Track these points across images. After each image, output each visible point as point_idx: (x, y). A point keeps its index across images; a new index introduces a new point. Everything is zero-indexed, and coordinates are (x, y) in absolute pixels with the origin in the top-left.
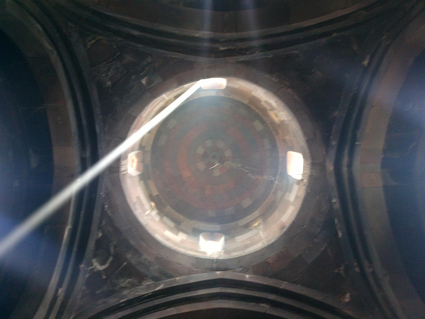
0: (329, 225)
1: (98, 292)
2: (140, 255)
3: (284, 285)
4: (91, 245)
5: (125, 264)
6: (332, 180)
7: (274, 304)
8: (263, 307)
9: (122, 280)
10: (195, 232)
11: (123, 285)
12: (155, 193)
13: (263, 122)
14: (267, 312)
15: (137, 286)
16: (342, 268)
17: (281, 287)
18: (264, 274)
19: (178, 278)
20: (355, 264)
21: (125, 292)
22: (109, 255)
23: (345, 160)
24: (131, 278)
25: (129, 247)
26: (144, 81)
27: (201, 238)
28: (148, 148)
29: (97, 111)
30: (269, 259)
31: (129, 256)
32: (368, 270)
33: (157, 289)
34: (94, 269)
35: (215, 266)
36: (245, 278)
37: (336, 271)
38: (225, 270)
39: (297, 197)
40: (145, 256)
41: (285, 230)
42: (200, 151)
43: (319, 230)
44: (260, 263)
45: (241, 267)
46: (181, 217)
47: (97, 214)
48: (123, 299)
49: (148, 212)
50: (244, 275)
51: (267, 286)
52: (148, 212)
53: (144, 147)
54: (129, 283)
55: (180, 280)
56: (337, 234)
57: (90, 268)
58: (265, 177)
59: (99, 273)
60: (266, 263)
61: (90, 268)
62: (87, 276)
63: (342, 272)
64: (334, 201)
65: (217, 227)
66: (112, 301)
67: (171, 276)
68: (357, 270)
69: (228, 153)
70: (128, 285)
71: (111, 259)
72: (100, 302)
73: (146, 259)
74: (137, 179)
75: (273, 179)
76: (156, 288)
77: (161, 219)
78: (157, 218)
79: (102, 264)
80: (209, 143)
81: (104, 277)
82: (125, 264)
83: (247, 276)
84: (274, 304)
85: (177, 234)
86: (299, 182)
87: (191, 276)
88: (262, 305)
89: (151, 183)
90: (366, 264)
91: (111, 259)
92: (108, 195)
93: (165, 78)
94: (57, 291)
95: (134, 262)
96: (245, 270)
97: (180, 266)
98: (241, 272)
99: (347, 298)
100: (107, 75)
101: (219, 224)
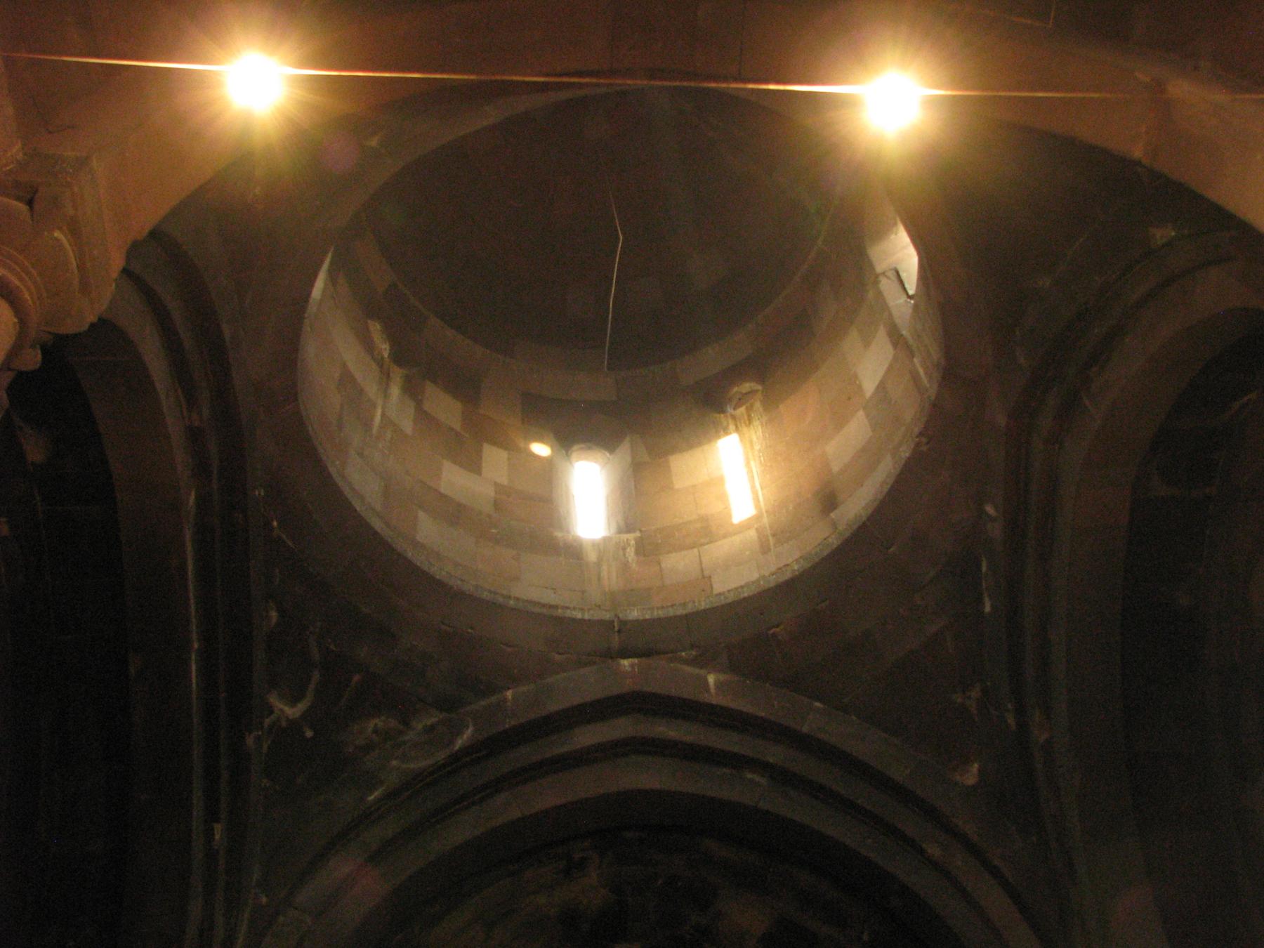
3: (814, 719)
5: (356, 678)
7: (782, 777)
14: (763, 805)
15: (401, 733)
16: (975, 693)
17: (805, 729)
19: (509, 694)
20: (1009, 706)
30: (777, 626)
33: (459, 743)
34: (279, 719)
35: (616, 641)
37: (958, 698)
43: (932, 574)
45: (692, 646)
50: (702, 672)
54: (376, 731)
56: (979, 601)
61: (267, 721)
68: (1011, 720)
71: (316, 676)
76: (451, 742)
79: (294, 701)
82: (356, 678)
84: (782, 777)
87: (549, 680)
88: (749, 776)
91: (316, 676)
94: (209, 833)
96: (705, 659)
97: (509, 650)
98: (692, 662)
99: (971, 776)
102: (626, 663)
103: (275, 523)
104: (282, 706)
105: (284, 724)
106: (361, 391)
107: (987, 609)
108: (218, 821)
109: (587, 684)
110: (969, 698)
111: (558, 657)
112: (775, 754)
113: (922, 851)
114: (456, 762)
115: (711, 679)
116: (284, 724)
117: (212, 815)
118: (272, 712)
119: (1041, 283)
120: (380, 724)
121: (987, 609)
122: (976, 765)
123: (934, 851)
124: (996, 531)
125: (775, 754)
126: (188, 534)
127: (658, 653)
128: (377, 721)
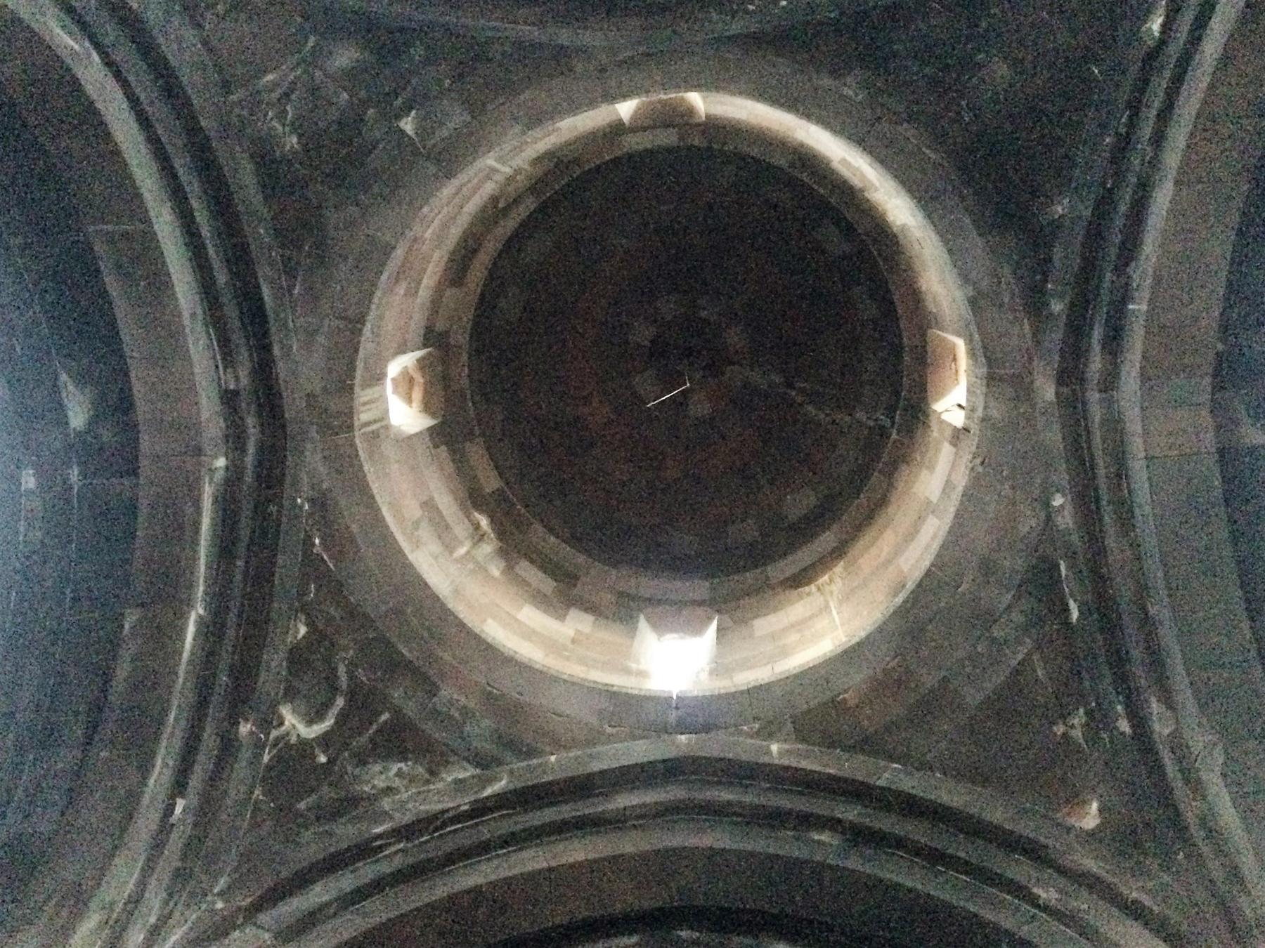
0: (1041, 582)
1: (302, 806)
2: (433, 691)
3: (890, 775)
4: (275, 661)
5: (385, 717)
6: (1054, 437)
7: (859, 836)
8: (819, 842)
9: (377, 768)
10: (623, 610)
11: (380, 783)
12: (491, 483)
13: (849, 230)
15: (428, 782)
16: (1079, 718)
18: (831, 742)
19: (553, 758)
21: (386, 804)
22: (334, 690)
23: (1096, 364)
24: (405, 760)
25: (395, 665)
26: (408, 125)
27: (643, 624)
28: (461, 338)
29: (260, 234)
30: (846, 691)
31: (397, 695)
32: (1161, 728)
33: (488, 792)
35: (673, 717)
36: (769, 753)
37: (1059, 729)
38: (706, 728)
39: (948, 485)
40: (447, 692)
41: (899, 600)
42: (643, 334)
44: (815, 709)
45: (756, 719)
46: (581, 559)
47: (287, 563)
48: (376, 822)
49: (462, 551)
50: (765, 743)
51: (832, 778)
52: (462, 551)
53: (445, 334)
55: (555, 764)
56: (1066, 610)
57: (274, 734)
58: (861, 415)
59: (305, 748)
60: (836, 705)
61: (274, 734)
62: (266, 758)
63: (1077, 734)
64: (1058, 501)
65: (700, 588)
66: (346, 833)
67: (531, 753)
68: (1124, 726)
69: (735, 338)
70: (397, 782)
71: (340, 702)
72: (307, 835)
73: (451, 703)
74: (422, 448)
75: (888, 423)
76: (484, 788)
77: (509, 569)
78: (496, 570)
80: (668, 307)
81: (323, 759)
82: (385, 717)
83: (774, 748)
84: (859, 836)
85: (561, 617)
86: (958, 435)
89: (476, 453)
90: (1155, 707)
91: (340, 702)
92: (321, 503)
93: (476, 108)
95: (410, 709)
96: (768, 731)
99: (1090, 818)
100: (282, 115)
101: (706, 577)
102: (683, 738)
103: (317, 541)
104: (294, 721)
105: (293, 740)
106: (447, 527)
107: (1075, 615)
108: (183, 797)
109: (641, 751)
110: (1072, 726)
111: (609, 730)
112: (851, 813)
113: (1034, 901)
114: (480, 810)
115: (774, 748)
116: (293, 740)
117: (179, 786)
118: (281, 724)
119: (1060, 209)
120: (405, 768)
121: (1075, 615)
122: (1095, 805)
123: (1047, 894)
124: (1066, 520)
125: (851, 813)
126: (208, 493)
127: (718, 728)
128: (402, 765)
